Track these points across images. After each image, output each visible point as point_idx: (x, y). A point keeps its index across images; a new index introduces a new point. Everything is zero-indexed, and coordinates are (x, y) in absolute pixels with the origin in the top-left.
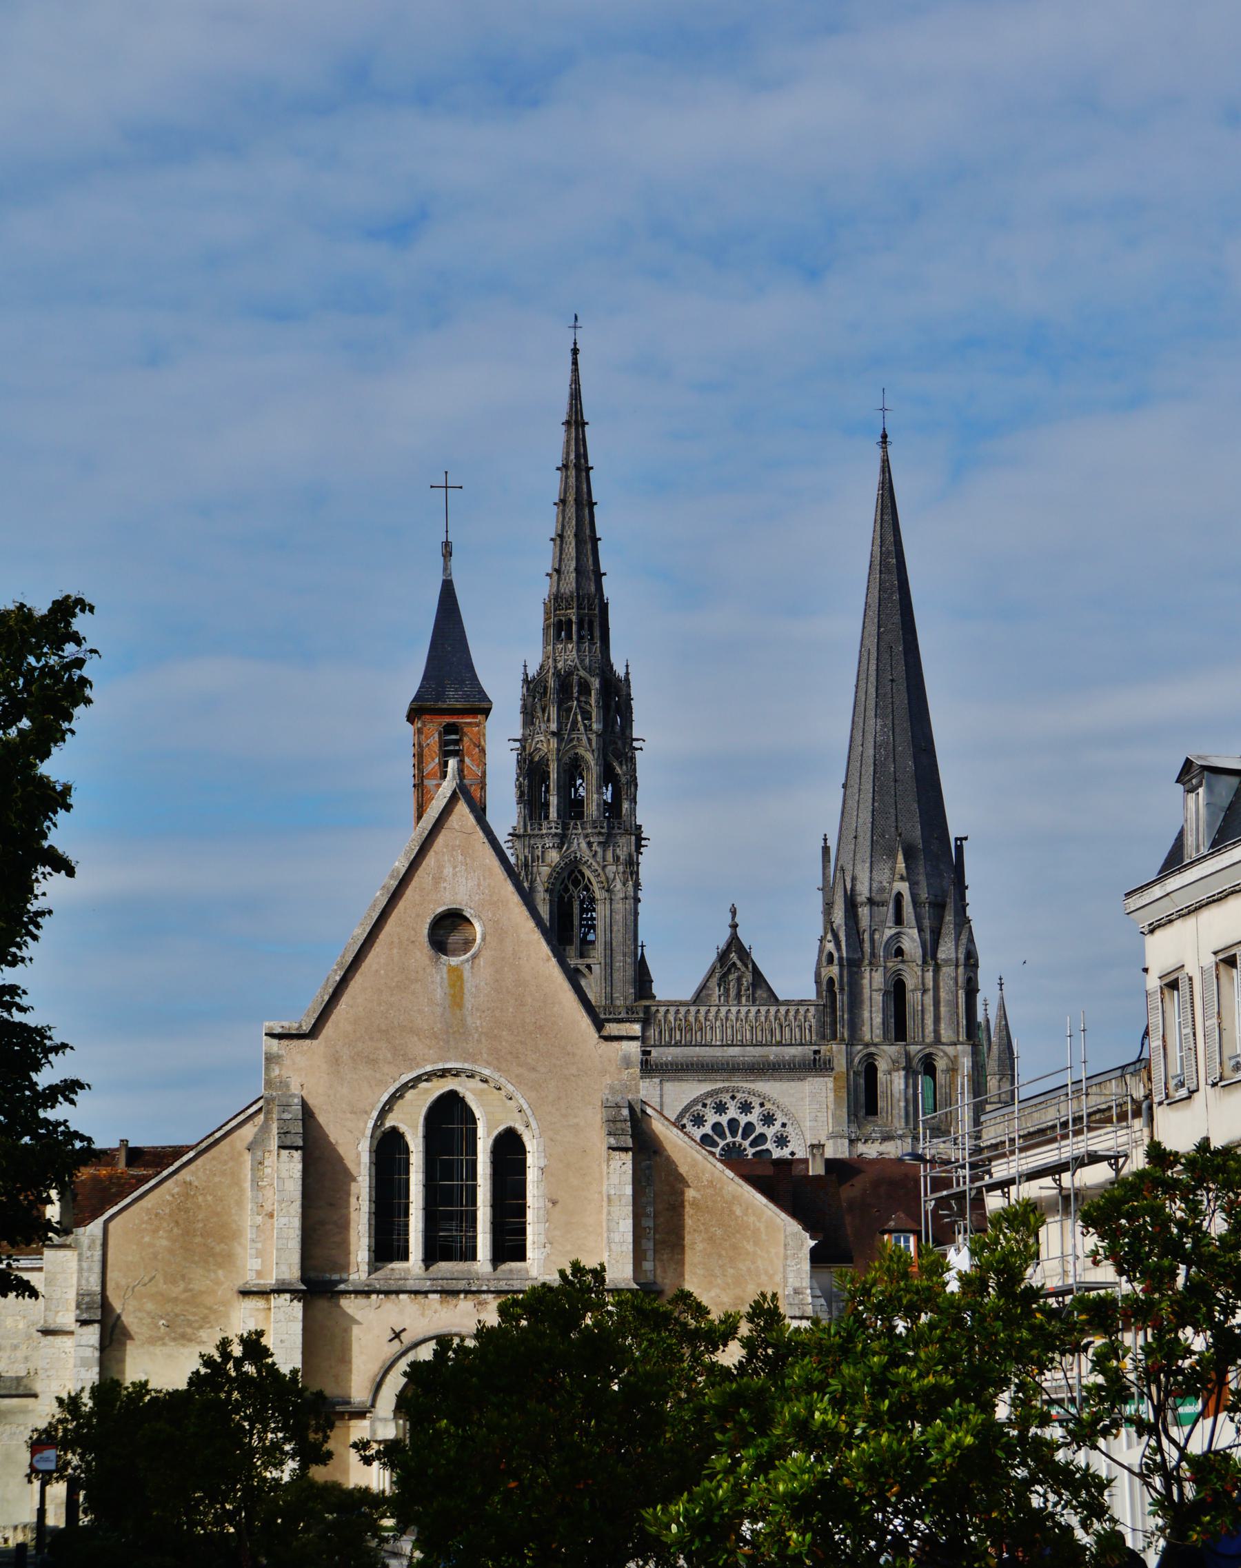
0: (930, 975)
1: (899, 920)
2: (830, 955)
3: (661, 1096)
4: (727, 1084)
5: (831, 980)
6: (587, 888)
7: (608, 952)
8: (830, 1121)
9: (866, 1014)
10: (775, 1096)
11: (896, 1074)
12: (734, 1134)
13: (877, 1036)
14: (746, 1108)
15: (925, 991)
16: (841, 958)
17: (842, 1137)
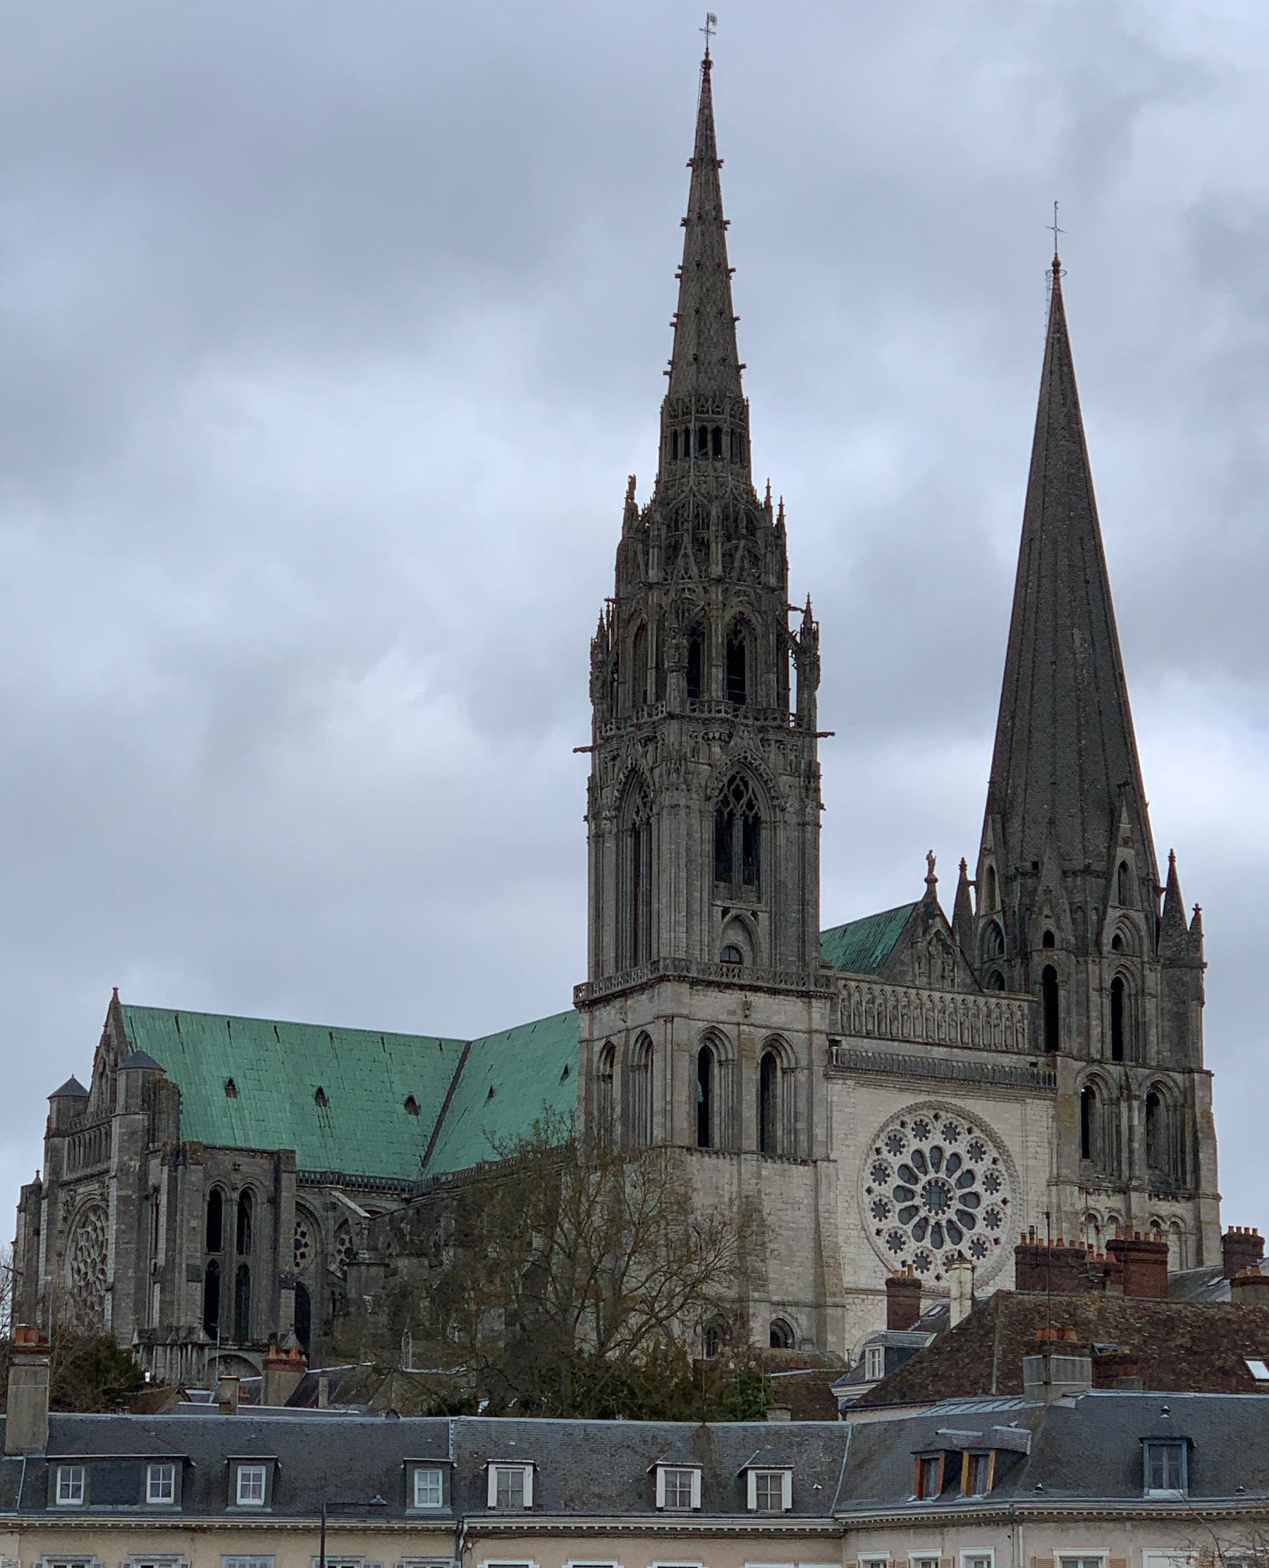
2: (1049, 940)
4: (933, 1098)
6: (750, 806)
10: (987, 1119)
12: (937, 1167)
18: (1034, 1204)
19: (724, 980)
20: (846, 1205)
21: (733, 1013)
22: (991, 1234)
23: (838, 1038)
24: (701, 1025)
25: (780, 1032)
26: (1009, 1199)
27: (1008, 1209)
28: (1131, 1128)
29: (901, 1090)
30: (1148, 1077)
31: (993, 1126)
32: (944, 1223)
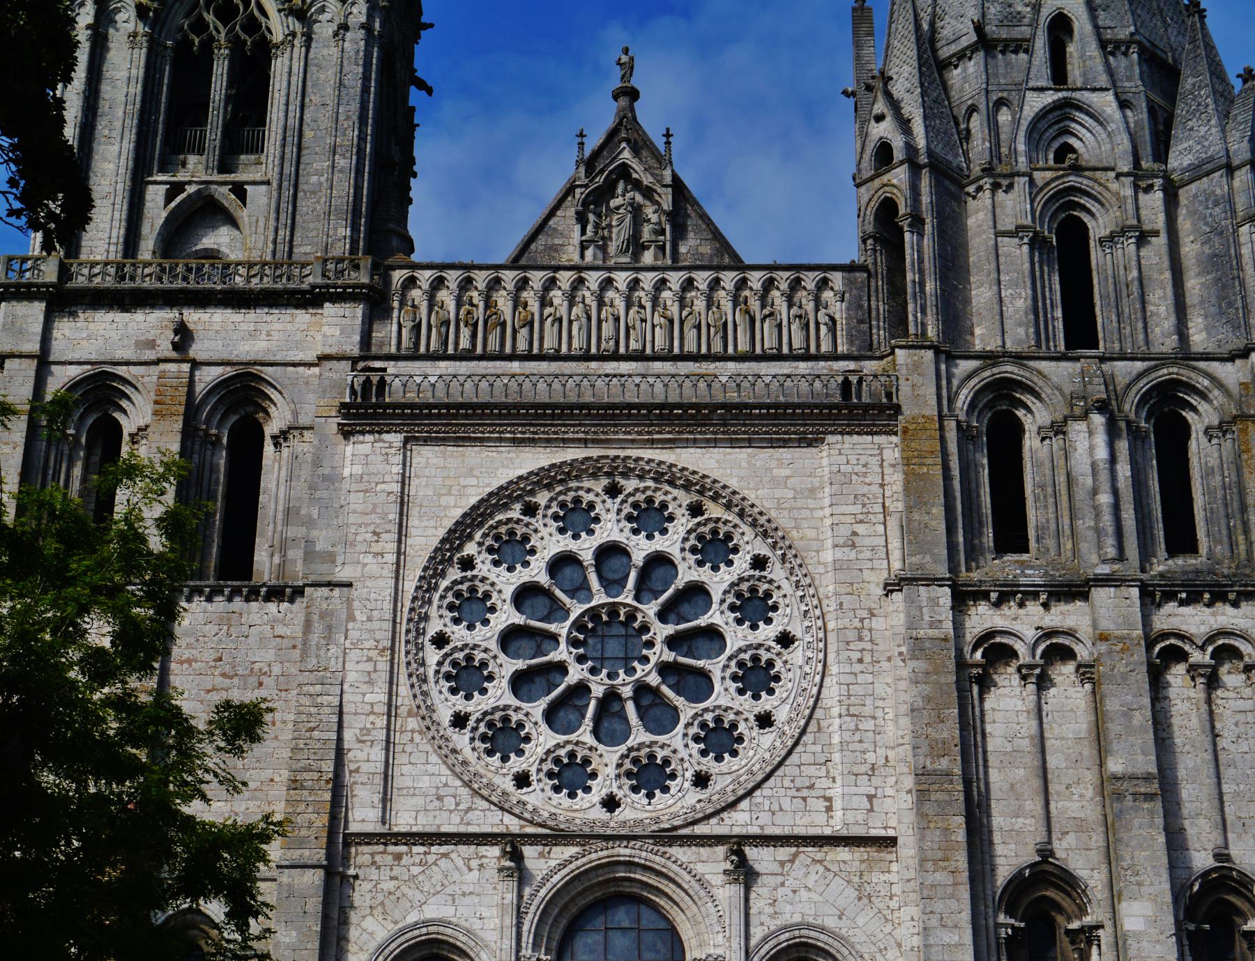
0: (1154, 201)
1: (1059, 75)
3: (404, 481)
4: (594, 452)
5: (887, 208)
6: (253, 26)
7: (291, 151)
8: (895, 544)
9: (980, 295)
10: (734, 483)
11: (1077, 430)
13: (1019, 342)
14: (649, 517)
15: (1143, 238)
16: (910, 148)
17: (931, 581)
18: (852, 635)
19: (128, 284)
20: (369, 667)
21: (152, 344)
22: (745, 703)
23: (378, 364)
24: (74, 372)
25: (255, 370)
26: (796, 630)
27: (797, 655)
28: (1094, 465)
29: (516, 442)
30: (1140, 375)
31: (752, 497)
32: (627, 692)
